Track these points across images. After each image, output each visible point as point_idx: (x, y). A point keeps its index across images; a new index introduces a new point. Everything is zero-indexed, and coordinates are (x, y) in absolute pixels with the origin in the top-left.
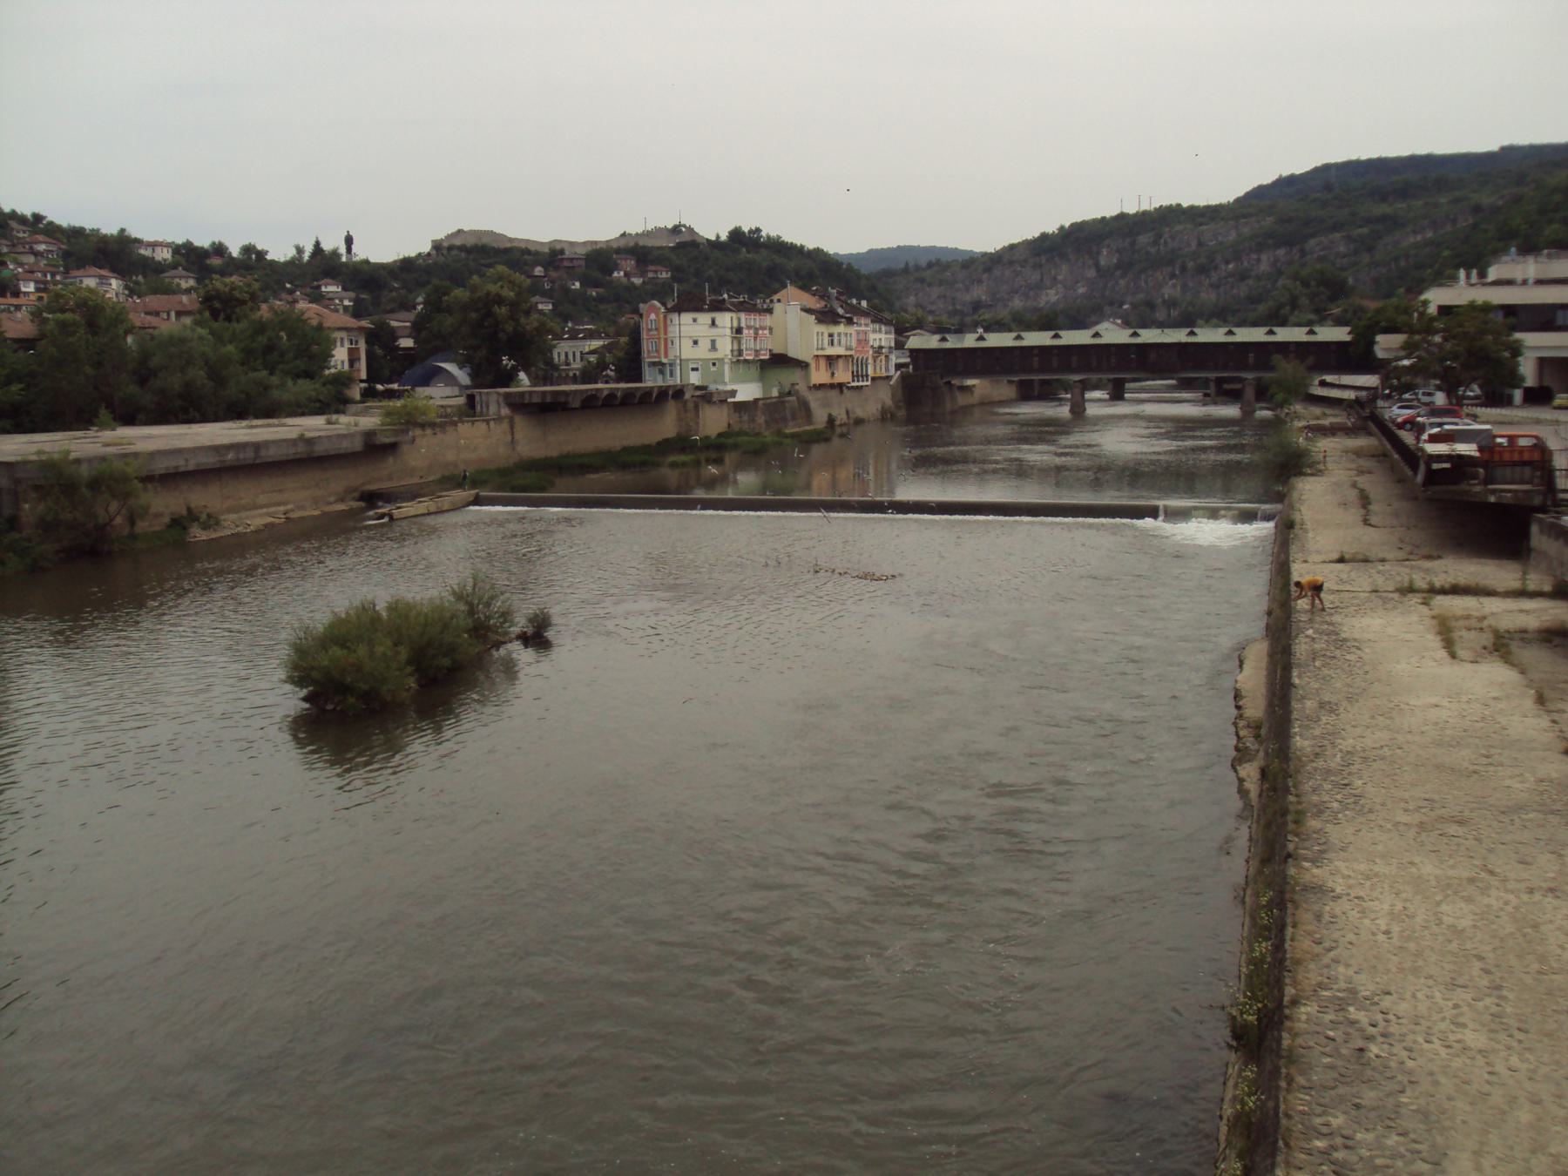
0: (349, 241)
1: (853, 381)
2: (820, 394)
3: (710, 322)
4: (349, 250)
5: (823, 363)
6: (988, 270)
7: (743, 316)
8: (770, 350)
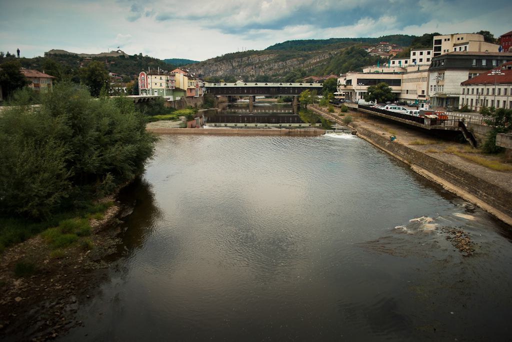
0: (18, 51)
2: (188, 99)
4: (18, 54)
5: (189, 90)
6: (203, 66)
7: (169, 76)
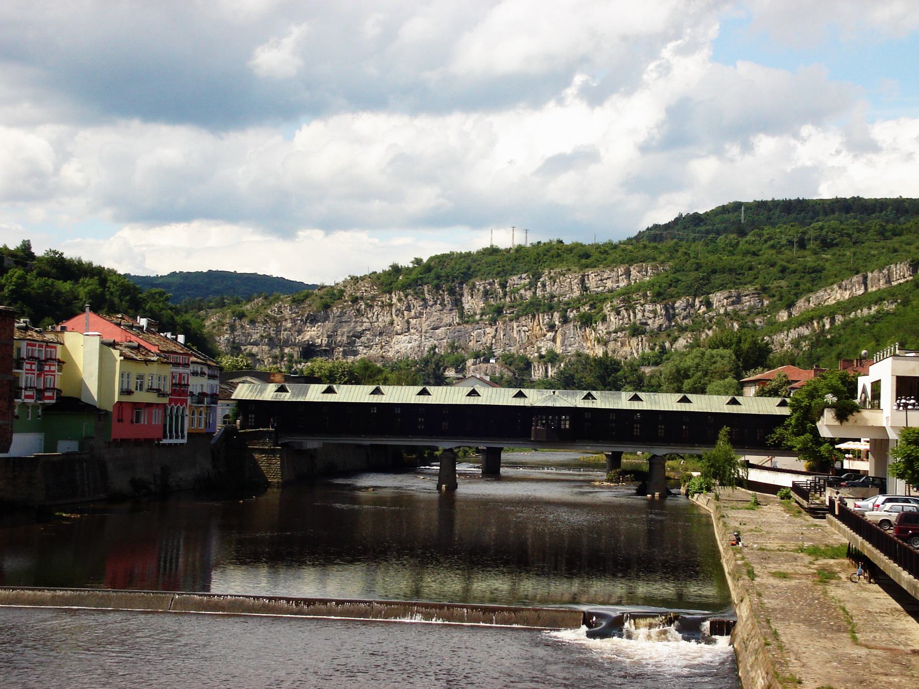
1: (165, 437)
8: (59, 391)
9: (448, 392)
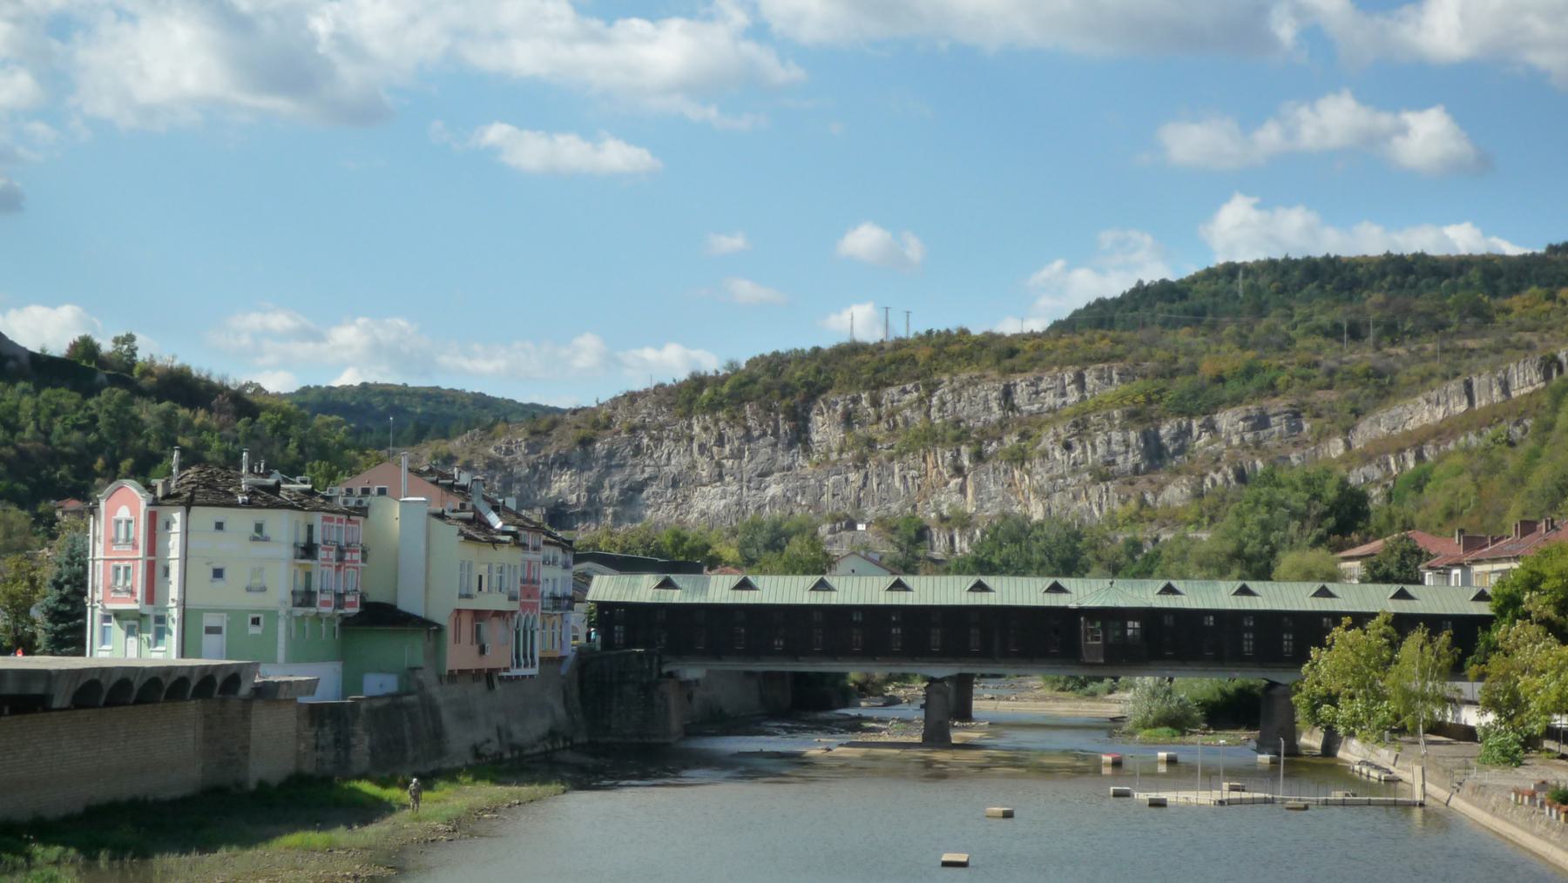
1: (518, 665)
3: (252, 530)
5: (466, 626)
7: (317, 519)
9: (937, 586)
